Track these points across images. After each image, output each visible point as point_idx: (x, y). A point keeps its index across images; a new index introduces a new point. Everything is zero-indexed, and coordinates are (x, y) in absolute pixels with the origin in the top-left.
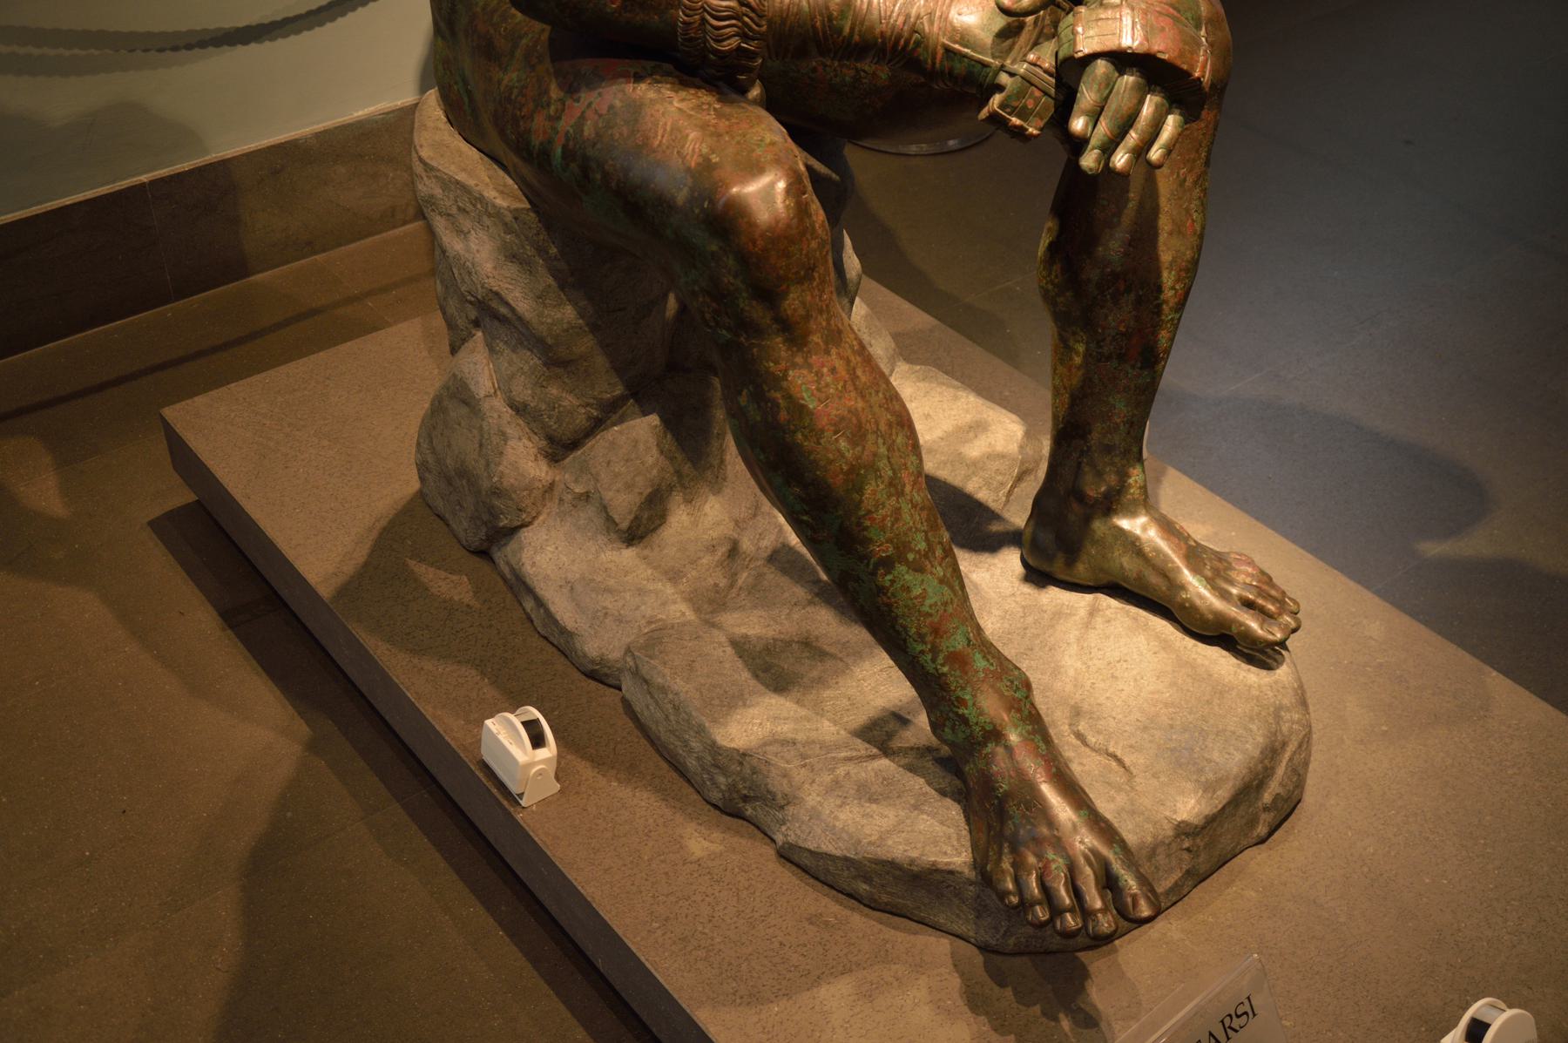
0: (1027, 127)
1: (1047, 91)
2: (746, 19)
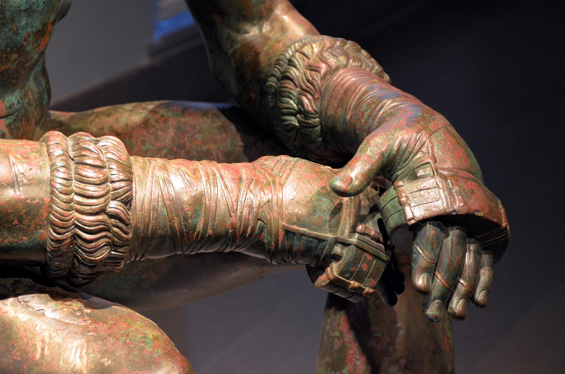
0: (364, 287)
1: (376, 254)
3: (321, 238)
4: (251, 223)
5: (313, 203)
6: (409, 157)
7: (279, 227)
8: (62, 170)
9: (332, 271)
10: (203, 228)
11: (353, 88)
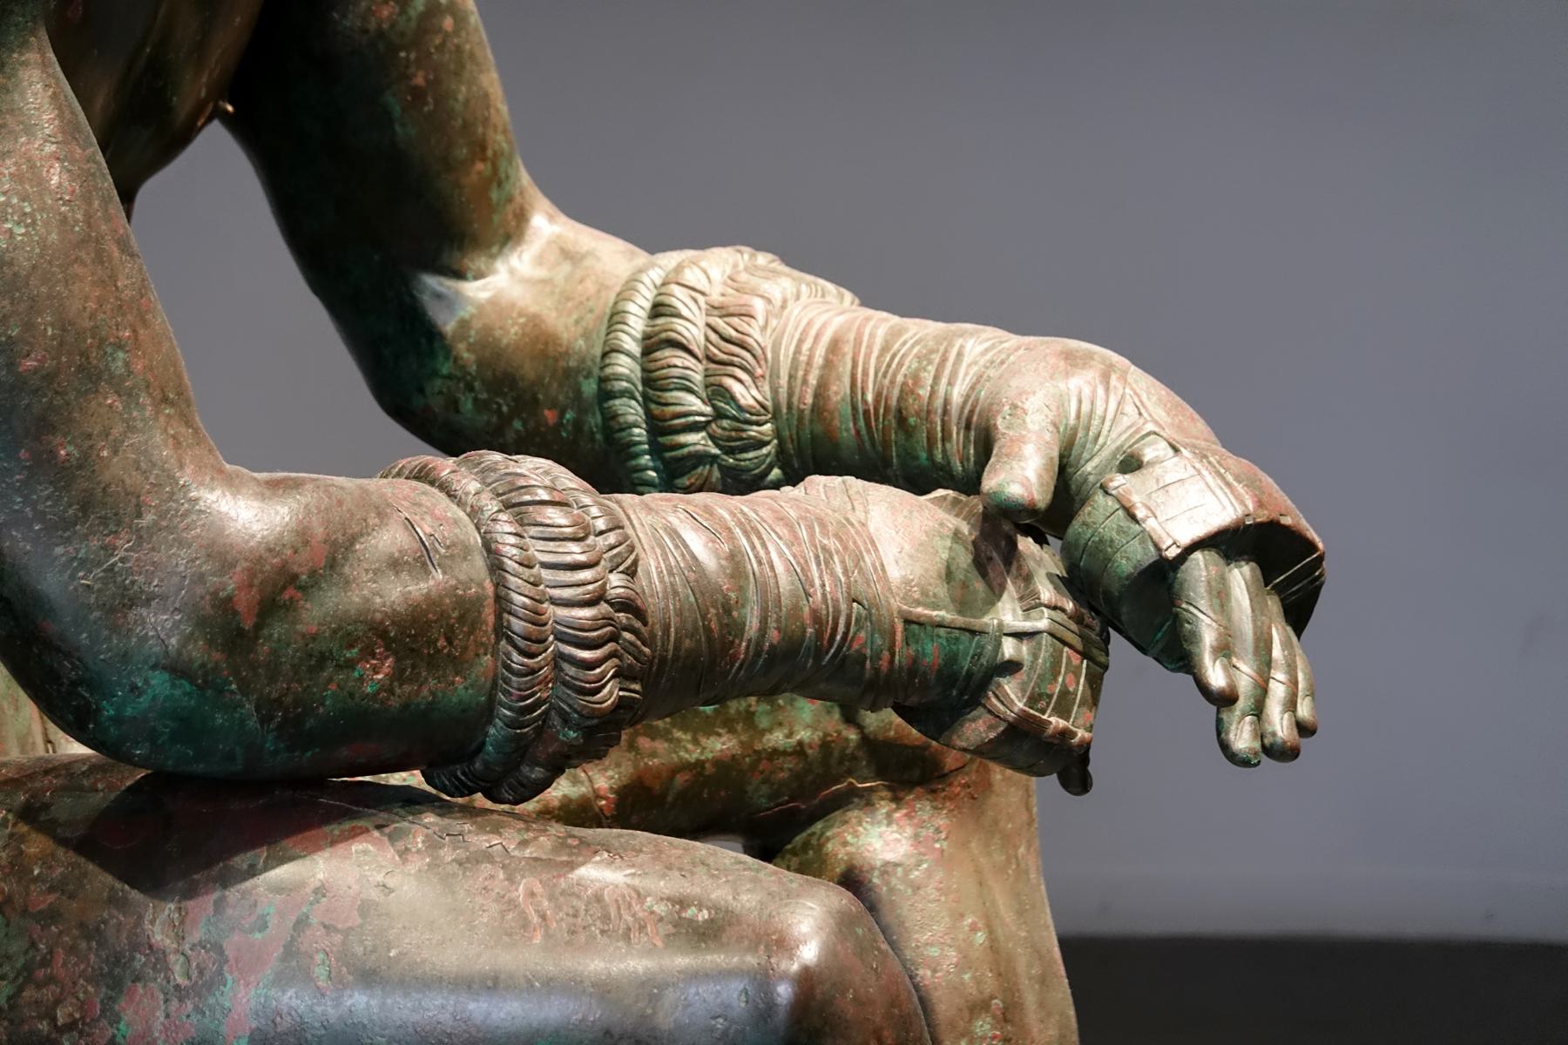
4: (843, 607)
8: (503, 517)
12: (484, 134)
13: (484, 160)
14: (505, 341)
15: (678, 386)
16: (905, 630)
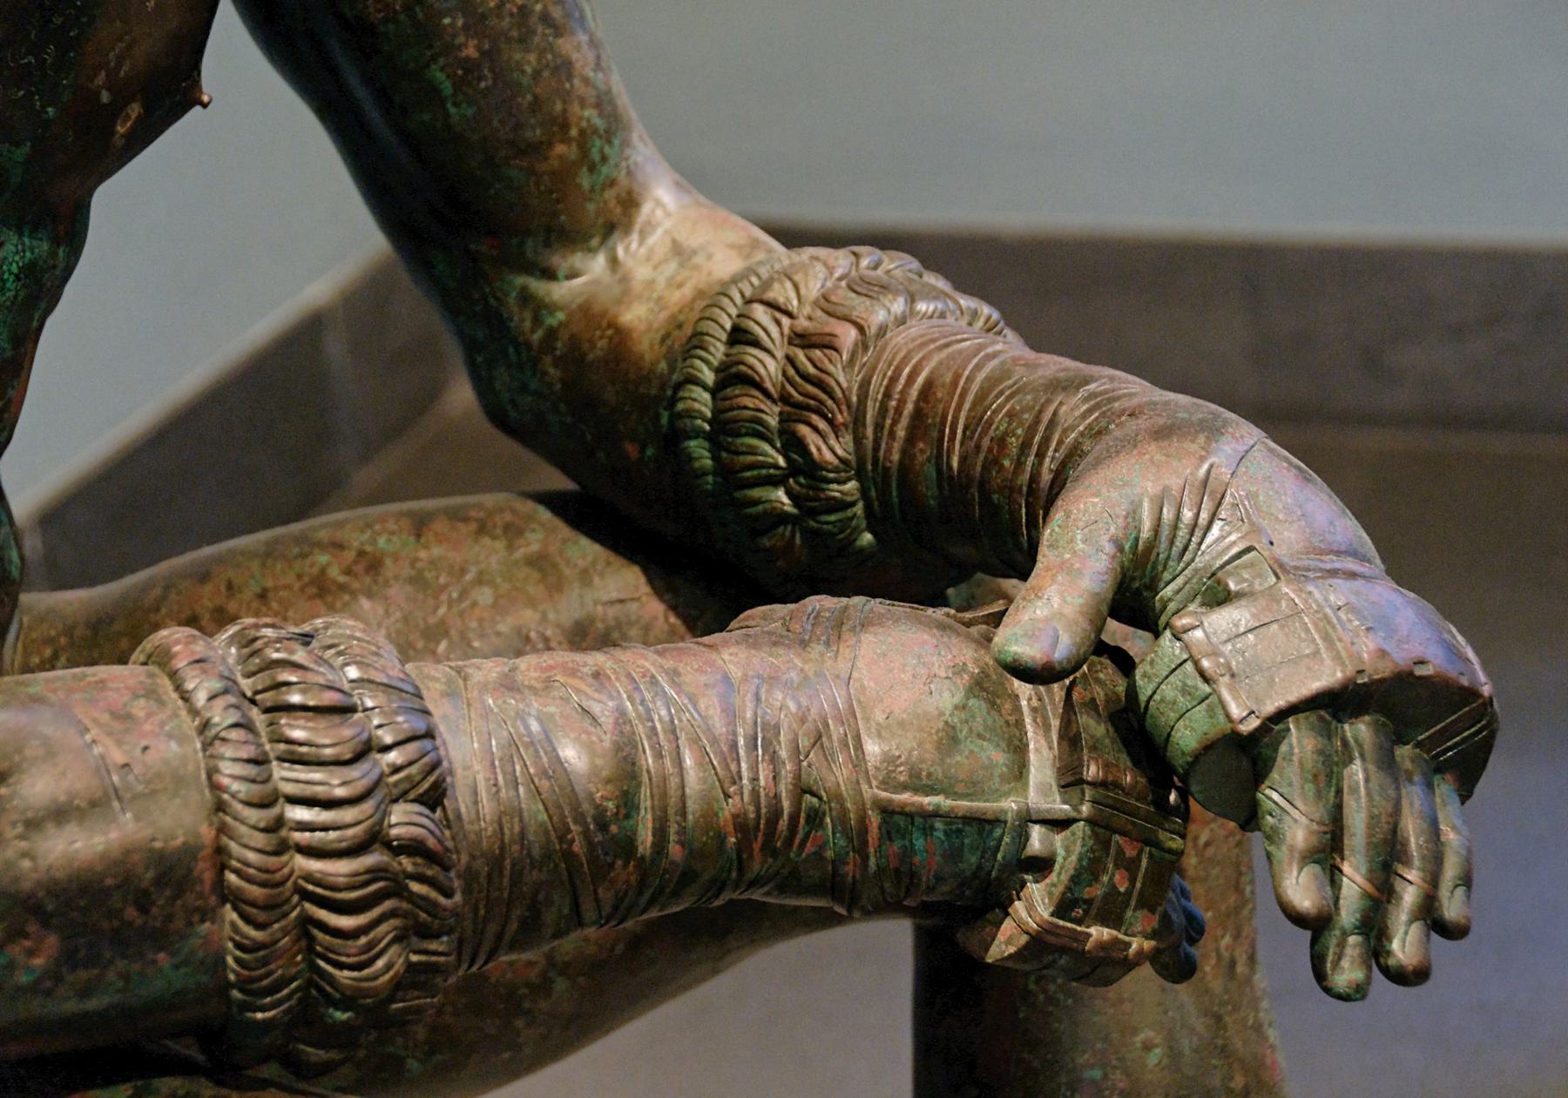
0: (1127, 939)
2: (415, 887)
3: (989, 816)
4: (786, 804)
5: (945, 718)
6: (1190, 540)
7: (864, 804)
8: (234, 734)
9: (1030, 908)
10: (654, 844)
11: (948, 378)
12: (565, 111)
13: (566, 140)
14: (591, 356)
15: (750, 431)
16: (884, 821)
